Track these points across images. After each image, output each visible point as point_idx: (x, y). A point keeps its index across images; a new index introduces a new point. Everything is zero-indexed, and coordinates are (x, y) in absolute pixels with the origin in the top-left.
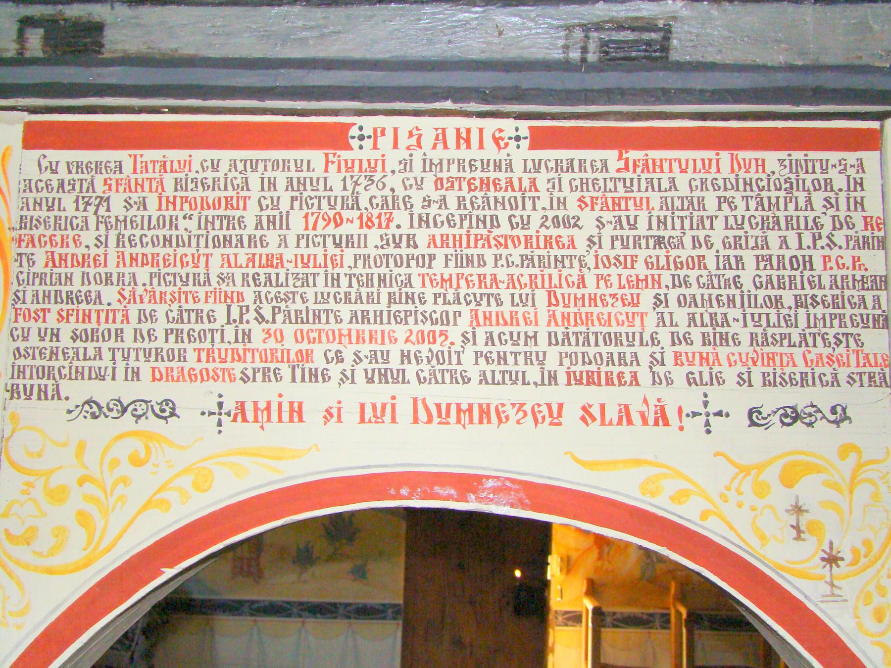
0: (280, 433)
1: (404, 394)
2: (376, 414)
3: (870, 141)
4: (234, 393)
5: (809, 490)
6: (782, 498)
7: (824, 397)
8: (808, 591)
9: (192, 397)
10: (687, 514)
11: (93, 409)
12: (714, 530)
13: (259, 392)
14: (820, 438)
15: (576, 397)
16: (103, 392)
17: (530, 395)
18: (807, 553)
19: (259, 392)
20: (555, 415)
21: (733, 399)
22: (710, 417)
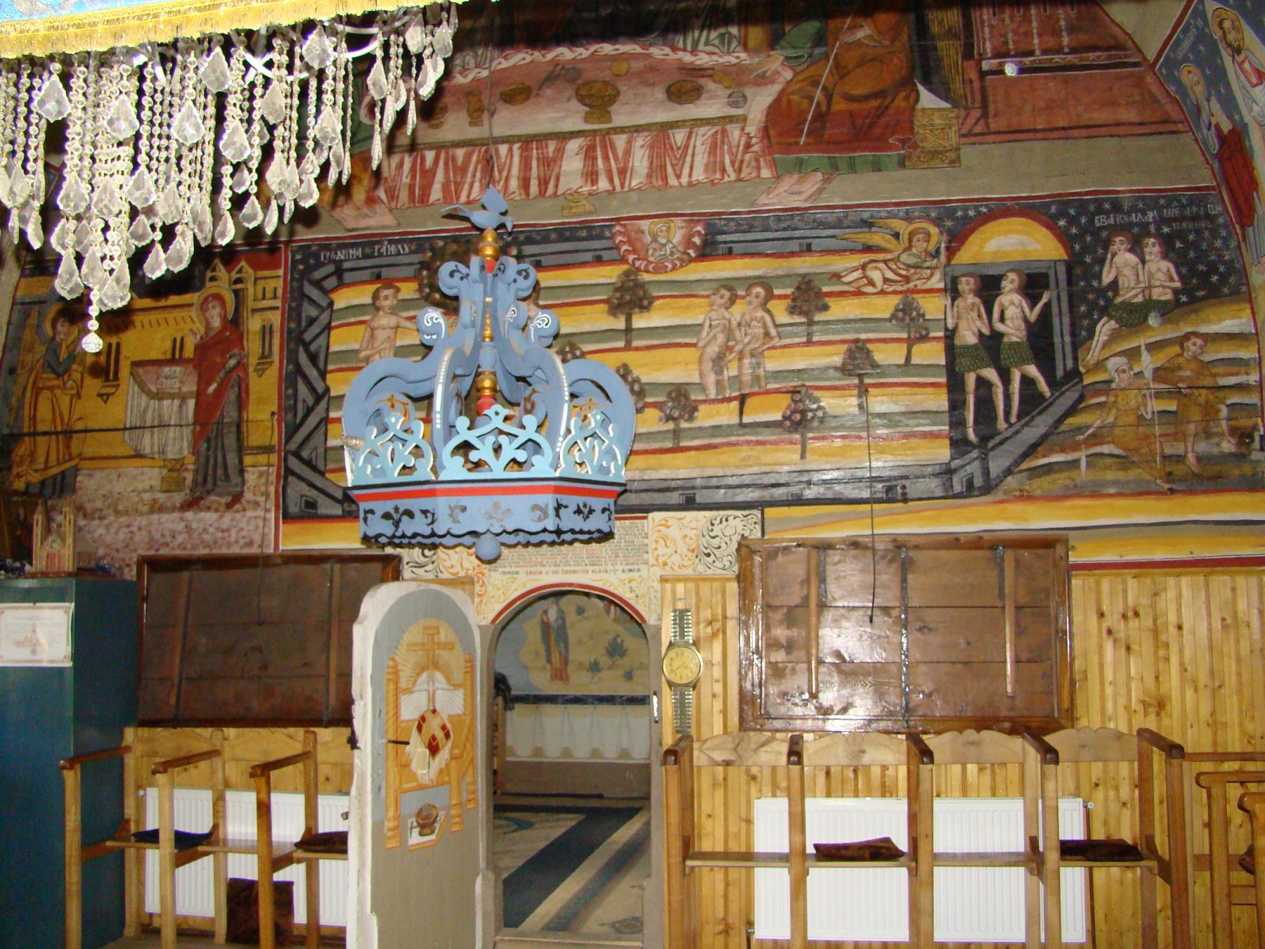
0: (538, 577)
1: (560, 569)
2: (555, 572)
3: (645, 518)
4: (529, 569)
5: (633, 584)
6: (628, 585)
7: (636, 567)
8: (632, 602)
9: (522, 570)
10: (611, 589)
11: (504, 573)
12: (616, 592)
13: (534, 569)
14: (635, 575)
15: (591, 568)
16: (506, 570)
17: (583, 568)
18: (632, 595)
19: (534, 569)
20: (587, 572)
21: (619, 568)
22: (615, 571)
